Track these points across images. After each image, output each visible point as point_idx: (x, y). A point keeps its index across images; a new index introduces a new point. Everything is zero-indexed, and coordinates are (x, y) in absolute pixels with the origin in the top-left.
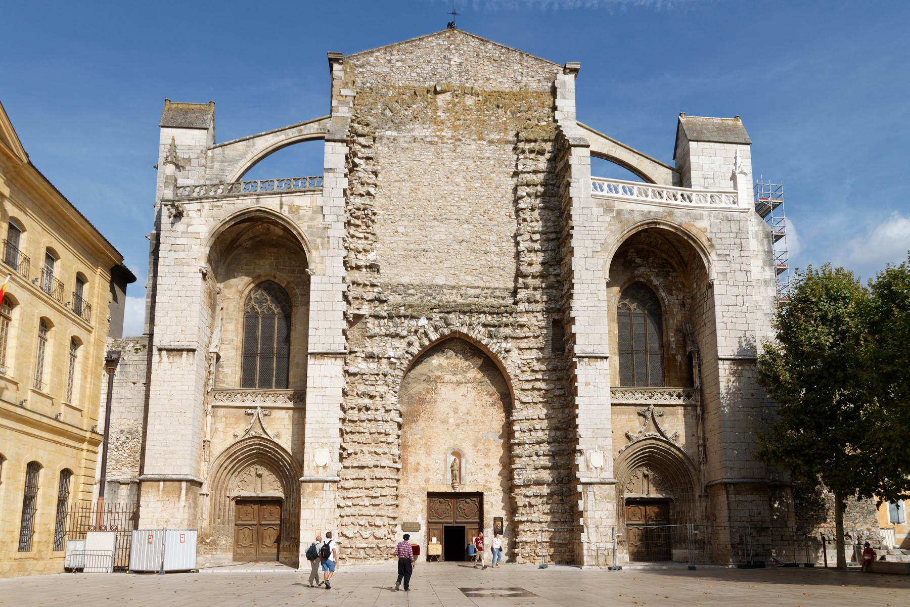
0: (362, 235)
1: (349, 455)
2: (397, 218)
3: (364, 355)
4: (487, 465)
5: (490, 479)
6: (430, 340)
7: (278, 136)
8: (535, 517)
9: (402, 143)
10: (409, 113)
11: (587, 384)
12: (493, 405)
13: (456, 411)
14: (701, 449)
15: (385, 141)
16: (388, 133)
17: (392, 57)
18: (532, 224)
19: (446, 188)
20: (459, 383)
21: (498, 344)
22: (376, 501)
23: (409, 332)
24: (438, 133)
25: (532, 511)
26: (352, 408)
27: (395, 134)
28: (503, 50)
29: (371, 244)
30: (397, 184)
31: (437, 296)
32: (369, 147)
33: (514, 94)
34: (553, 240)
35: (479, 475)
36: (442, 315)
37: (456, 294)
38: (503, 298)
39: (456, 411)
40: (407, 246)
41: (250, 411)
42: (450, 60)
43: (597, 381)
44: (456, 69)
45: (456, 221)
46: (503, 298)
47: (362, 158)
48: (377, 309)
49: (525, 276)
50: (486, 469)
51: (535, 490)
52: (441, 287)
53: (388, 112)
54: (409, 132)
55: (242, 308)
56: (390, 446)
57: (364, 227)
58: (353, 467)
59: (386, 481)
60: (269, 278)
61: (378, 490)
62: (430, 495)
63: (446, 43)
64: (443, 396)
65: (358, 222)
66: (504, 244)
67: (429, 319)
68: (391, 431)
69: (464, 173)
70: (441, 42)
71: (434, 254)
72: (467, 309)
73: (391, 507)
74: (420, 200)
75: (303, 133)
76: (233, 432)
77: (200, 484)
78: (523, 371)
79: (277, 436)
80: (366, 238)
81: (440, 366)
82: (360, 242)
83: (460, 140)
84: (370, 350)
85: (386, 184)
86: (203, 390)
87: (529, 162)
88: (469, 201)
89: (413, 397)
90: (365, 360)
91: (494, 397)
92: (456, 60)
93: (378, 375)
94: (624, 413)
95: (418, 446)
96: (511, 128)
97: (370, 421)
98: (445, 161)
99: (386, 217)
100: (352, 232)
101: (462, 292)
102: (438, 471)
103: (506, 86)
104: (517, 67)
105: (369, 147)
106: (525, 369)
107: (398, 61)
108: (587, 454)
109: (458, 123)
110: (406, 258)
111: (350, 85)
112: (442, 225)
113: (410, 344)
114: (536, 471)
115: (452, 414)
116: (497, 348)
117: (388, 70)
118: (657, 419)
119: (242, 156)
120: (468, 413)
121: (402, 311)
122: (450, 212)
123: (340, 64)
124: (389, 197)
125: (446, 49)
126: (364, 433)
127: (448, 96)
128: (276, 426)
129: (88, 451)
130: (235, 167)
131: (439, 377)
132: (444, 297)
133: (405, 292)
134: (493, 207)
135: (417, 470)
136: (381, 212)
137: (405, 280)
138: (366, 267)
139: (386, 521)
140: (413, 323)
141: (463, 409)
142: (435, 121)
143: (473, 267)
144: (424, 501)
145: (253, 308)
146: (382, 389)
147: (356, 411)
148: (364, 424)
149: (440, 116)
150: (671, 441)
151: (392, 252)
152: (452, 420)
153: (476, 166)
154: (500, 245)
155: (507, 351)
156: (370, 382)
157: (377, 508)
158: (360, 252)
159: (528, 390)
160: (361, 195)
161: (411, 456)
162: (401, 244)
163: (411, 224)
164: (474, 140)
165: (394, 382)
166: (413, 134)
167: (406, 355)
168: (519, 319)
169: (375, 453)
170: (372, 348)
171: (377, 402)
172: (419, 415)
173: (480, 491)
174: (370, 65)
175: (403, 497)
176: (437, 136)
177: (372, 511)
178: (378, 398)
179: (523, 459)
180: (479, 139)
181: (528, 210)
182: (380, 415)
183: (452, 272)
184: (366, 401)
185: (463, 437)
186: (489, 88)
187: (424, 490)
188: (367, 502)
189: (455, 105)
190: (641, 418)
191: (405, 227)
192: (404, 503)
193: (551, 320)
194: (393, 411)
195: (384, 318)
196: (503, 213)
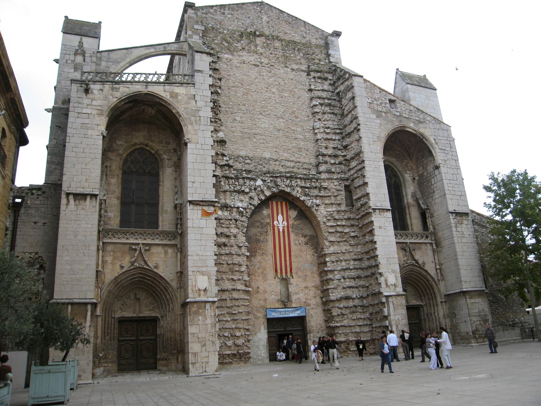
2: (235, 111)
4: (306, 287)
5: (309, 298)
6: (265, 196)
7: (149, 49)
8: (345, 323)
10: (239, 45)
11: (380, 227)
12: (306, 244)
14: (438, 271)
16: (226, 56)
17: (225, 11)
19: (267, 94)
21: (311, 201)
23: (251, 190)
24: (259, 60)
25: (343, 319)
27: (230, 57)
28: (294, 18)
29: (219, 127)
30: (233, 89)
31: (266, 166)
33: (303, 44)
34: (338, 133)
35: (301, 294)
40: (243, 130)
41: (134, 247)
42: (262, 18)
43: (386, 225)
49: (324, 155)
54: (240, 57)
55: (121, 167)
60: (142, 146)
61: (236, 308)
63: (258, 8)
66: (306, 134)
67: (264, 181)
69: (277, 87)
70: (256, 7)
71: (262, 137)
72: (288, 175)
74: (250, 100)
75: (167, 49)
76: (120, 263)
78: (329, 220)
79: (156, 267)
83: (273, 66)
84: (224, 201)
85: (226, 88)
87: (319, 85)
88: (282, 104)
92: (265, 18)
93: (231, 220)
97: (227, 254)
101: (282, 164)
102: (273, 293)
103: (297, 39)
106: (329, 218)
108: (386, 275)
110: (242, 138)
111: (200, 23)
112: (265, 118)
113: (251, 198)
114: (344, 290)
116: (310, 203)
117: (222, 18)
118: (413, 252)
123: (193, 9)
124: (229, 96)
125: (258, 12)
126: (223, 264)
128: (155, 259)
130: (117, 66)
135: (258, 292)
136: (224, 106)
137: (243, 153)
139: (243, 332)
142: (256, 52)
143: (288, 148)
146: (234, 231)
148: (223, 258)
149: (259, 50)
150: (422, 267)
151: (232, 133)
153: (285, 83)
155: (318, 205)
156: (225, 226)
159: (333, 232)
161: (252, 282)
163: (245, 116)
164: (282, 67)
166: (243, 58)
167: (250, 206)
168: (322, 184)
169: (232, 279)
170: (225, 200)
171: (232, 241)
172: (256, 251)
174: (211, 14)
178: (232, 238)
179: (335, 282)
180: (285, 67)
181: (320, 113)
182: (235, 250)
183: (274, 150)
186: (287, 38)
190: (403, 252)
191: (241, 117)
193: (344, 185)
195: (232, 178)
196: (304, 114)
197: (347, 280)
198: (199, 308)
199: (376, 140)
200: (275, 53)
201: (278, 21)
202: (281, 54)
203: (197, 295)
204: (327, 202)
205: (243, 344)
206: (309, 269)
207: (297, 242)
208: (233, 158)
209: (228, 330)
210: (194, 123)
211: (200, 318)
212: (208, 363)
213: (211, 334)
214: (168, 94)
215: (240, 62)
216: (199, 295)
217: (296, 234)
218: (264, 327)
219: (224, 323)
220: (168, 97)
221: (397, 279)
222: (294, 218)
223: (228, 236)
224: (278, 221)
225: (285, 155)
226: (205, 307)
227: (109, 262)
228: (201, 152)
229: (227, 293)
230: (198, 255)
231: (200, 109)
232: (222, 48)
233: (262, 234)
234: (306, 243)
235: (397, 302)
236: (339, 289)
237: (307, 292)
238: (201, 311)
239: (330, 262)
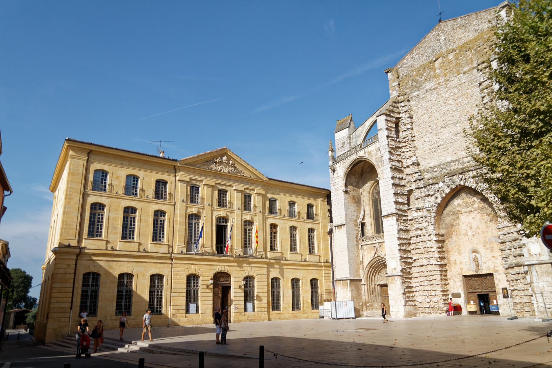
0: (408, 150)
1: (415, 260)
3: (415, 209)
4: (493, 257)
12: (491, 220)
13: (471, 228)
15: (414, 99)
16: (415, 94)
20: (470, 212)
22: (431, 283)
23: (435, 192)
24: (437, 82)
26: (413, 237)
27: (418, 93)
28: (466, 18)
32: (405, 106)
35: (490, 263)
36: (450, 178)
37: (458, 164)
39: (471, 228)
40: (430, 147)
42: (440, 40)
45: (452, 124)
46: (469, 162)
47: (403, 113)
48: (419, 184)
50: (493, 259)
51: (517, 270)
52: (450, 162)
53: (414, 84)
56: (434, 253)
57: (409, 145)
58: (418, 266)
59: (435, 272)
62: (465, 276)
63: (437, 32)
64: (462, 221)
65: (404, 144)
68: (433, 246)
69: (453, 97)
70: (434, 33)
71: (444, 146)
73: (439, 285)
74: (433, 121)
77: (361, 280)
80: (410, 151)
81: (459, 204)
82: (407, 153)
88: (458, 110)
91: (491, 216)
95: (454, 250)
96: (475, 59)
97: (422, 242)
98: (442, 95)
99: (419, 136)
100: (403, 150)
101: (461, 162)
103: (471, 36)
104: (475, 22)
105: (405, 106)
109: (446, 71)
110: (431, 153)
112: (445, 129)
114: (515, 258)
115: (469, 230)
119: (362, 132)
120: (478, 228)
121: (431, 182)
122: (449, 120)
124: (419, 125)
127: (440, 60)
129: (324, 270)
131: (459, 211)
132: (452, 167)
133: (432, 171)
134: (471, 108)
135: (455, 264)
137: (432, 165)
138: (411, 165)
140: (436, 186)
141: (474, 226)
142: (435, 77)
144: (461, 281)
145: (375, 197)
146: (425, 224)
147: (415, 238)
148: (420, 244)
152: (470, 234)
156: (419, 222)
157: (432, 286)
158: (408, 159)
160: (405, 131)
162: (428, 147)
165: (430, 219)
167: (434, 205)
172: (452, 233)
173: (492, 272)
175: (450, 279)
176: (437, 84)
177: (429, 288)
178: (424, 230)
179: (507, 252)
180: (458, 75)
182: (426, 238)
183: (454, 153)
184: (419, 232)
185: (477, 242)
186: (462, 43)
187: (460, 274)
188: (426, 283)
189: (444, 63)
191: (429, 137)
192: (451, 282)
194: (432, 235)
195: (422, 188)
198: (392, 280)
201: (453, 31)
205: (438, 301)
211: (393, 285)
215: (423, 93)
219: (424, 286)
223: (421, 230)
228: (386, 183)
229: (424, 267)
230: (390, 248)
233: (455, 220)
235: (541, 270)
236: (511, 258)
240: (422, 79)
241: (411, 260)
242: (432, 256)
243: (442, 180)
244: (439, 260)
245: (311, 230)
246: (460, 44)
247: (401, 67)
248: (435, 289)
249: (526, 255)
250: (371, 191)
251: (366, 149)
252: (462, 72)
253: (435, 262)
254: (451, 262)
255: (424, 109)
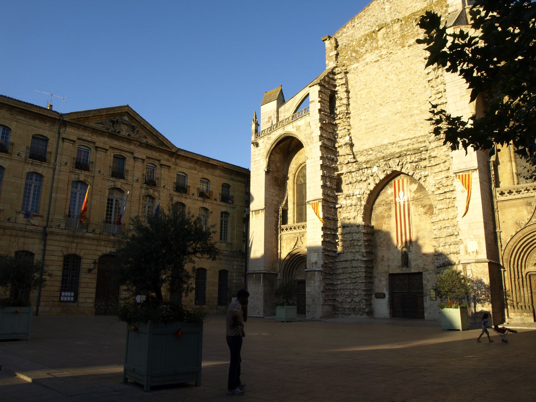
2: (361, 112)
5: (427, 263)
9: (361, 68)
10: (363, 50)
12: (426, 213)
15: (352, 71)
18: (437, 88)
30: (359, 93)
31: (384, 151)
35: (419, 261)
38: (425, 141)
42: (384, 9)
44: (388, 12)
45: (393, 102)
53: (354, 54)
57: (343, 123)
59: (359, 268)
69: (395, 72)
71: (382, 126)
73: (363, 284)
77: (276, 275)
85: (354, 95)
86: (274, 227)
88: (399, 87)
89: (378, 216)
90: (345, 199)
91: (426, 208)
94: (513, 206)
95: (383, 245)
101: (398, 145)
102: (395, 260)
106: (437, 186)
107: (358, 24)
119: (291, 106)
127: (383, 31)
133: (367, 154)
135: (383, 260)
137: (367, 147)
138: (345, 145)
140: (369, 171)
142: (377, 48)
143: (404, 127)
144: (387, 279)
153: (402, 64)
154: (420, 108)
157: (355, 284)
161: (379, 252)
163: (368, 113)
173: (420, 271)
174: (345, 33)
180: (402, 48)
181: (433, 80)
197: (451, 246)
198: (311, 275)
199: (465, 93)
200: (394, 38)
202: (399, 35)
203: (311, 266)
204: (437, 170)
206: (428, 237)
207: (416, 213)
208: (359, 153)
209: (349, 290)
210: (310, 144)
211: (312, 281)
212: (315, 312)
213: (318, 293)
214: (295, 129)
215: (363, 65)
216: (313, 266)
217: (416, 206)
218: (386, 289)
220: (295, 131)
221: (480, 246)
222: (414, 192)
224: (399, 197)
225: (403, 136)
226: (315, 274)
227: (284, 246)
229: (348, 263)
231: (313, 132)
232: (351, 61)
234: (425, 213)
235: (477, 270)
237: (425, 259)
238: (312, 277)
239: (437, 230)
240: (361, 51)
241: (334, 255)
242: (358, 250)
243: (377, 165)
244: (365, 255)
245: (225, 214)
246: (407, 15)
247: (340, 36)
248: (357, 287)
249: (462, 252)
250: (297, 174)
251: (295, 124)
252: (407, 45)
253: (360, 258)
254: (378, 258)
255: (363, 83)
